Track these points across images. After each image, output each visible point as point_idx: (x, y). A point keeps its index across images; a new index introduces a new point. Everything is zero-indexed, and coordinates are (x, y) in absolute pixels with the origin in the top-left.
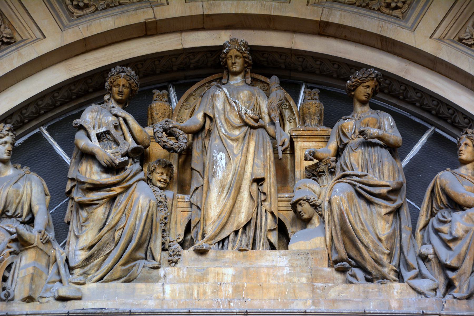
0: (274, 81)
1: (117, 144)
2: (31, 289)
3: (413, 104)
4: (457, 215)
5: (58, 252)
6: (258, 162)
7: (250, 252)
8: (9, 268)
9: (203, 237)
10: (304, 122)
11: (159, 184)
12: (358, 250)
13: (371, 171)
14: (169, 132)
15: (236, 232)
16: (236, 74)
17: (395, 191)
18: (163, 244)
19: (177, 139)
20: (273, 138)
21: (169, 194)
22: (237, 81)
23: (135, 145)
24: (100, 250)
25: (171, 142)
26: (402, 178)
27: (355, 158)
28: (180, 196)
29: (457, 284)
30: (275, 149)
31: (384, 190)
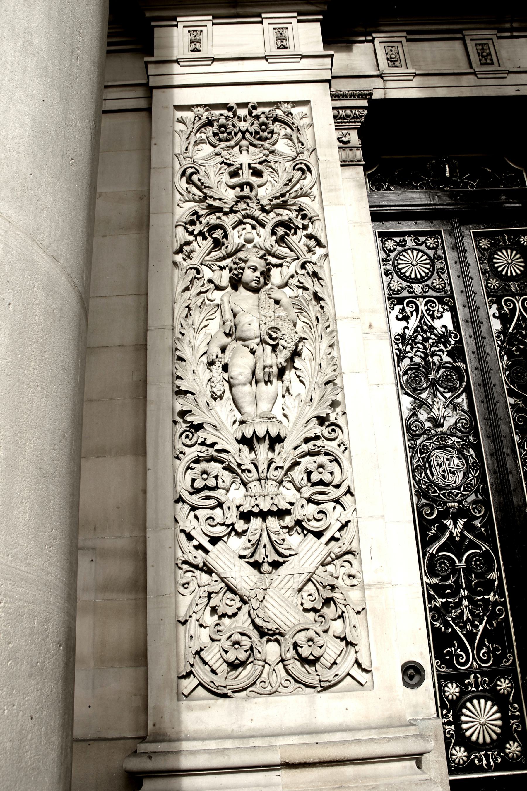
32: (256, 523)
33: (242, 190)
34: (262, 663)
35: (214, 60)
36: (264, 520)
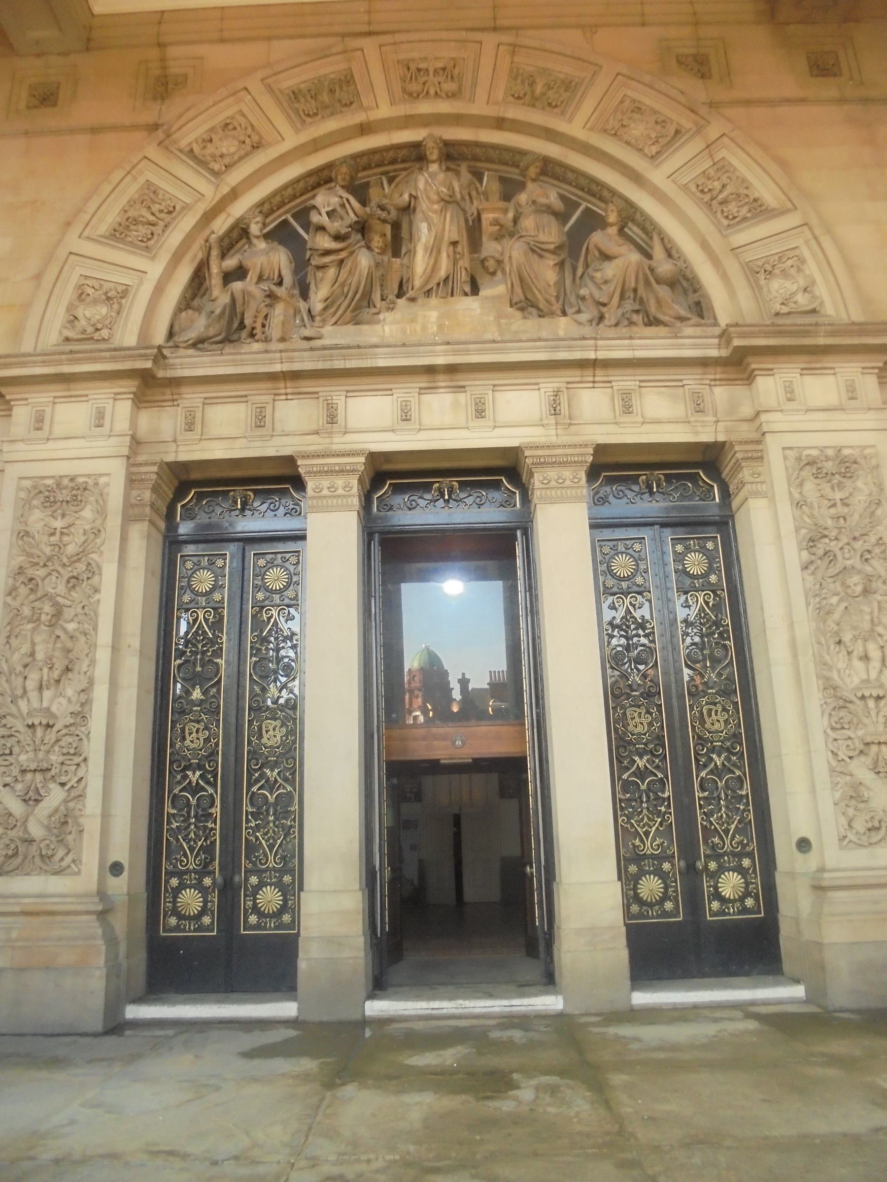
0: (464, 168)
1: (342, 218)
2: (283, 332)
3: (570, 184)
4: (606, 264)
5: (302, 305)
6: (454, 229)
7: (450, 299)
8: (266, 317)
9: (412, 289)
10: (487, 199)
11: (376, 250)
12: (533, 293)
13: (541, 232)
14: (382, 208)
15: (438, 284)
16: (433, 162)
17: (560, 248)
18: (382, 296)
19: (389, 213)
20: (464, 211)
21: (386, 258)
22: (434, 167)
23: (356, 219)
24: (333, 302)
25: (384, 215)
26: (565, 238)
27: (528, 223)
28: (394, 259)
29: (607, 316)
30: (466, 221)
31: (552, 247)
35: (807, 411)
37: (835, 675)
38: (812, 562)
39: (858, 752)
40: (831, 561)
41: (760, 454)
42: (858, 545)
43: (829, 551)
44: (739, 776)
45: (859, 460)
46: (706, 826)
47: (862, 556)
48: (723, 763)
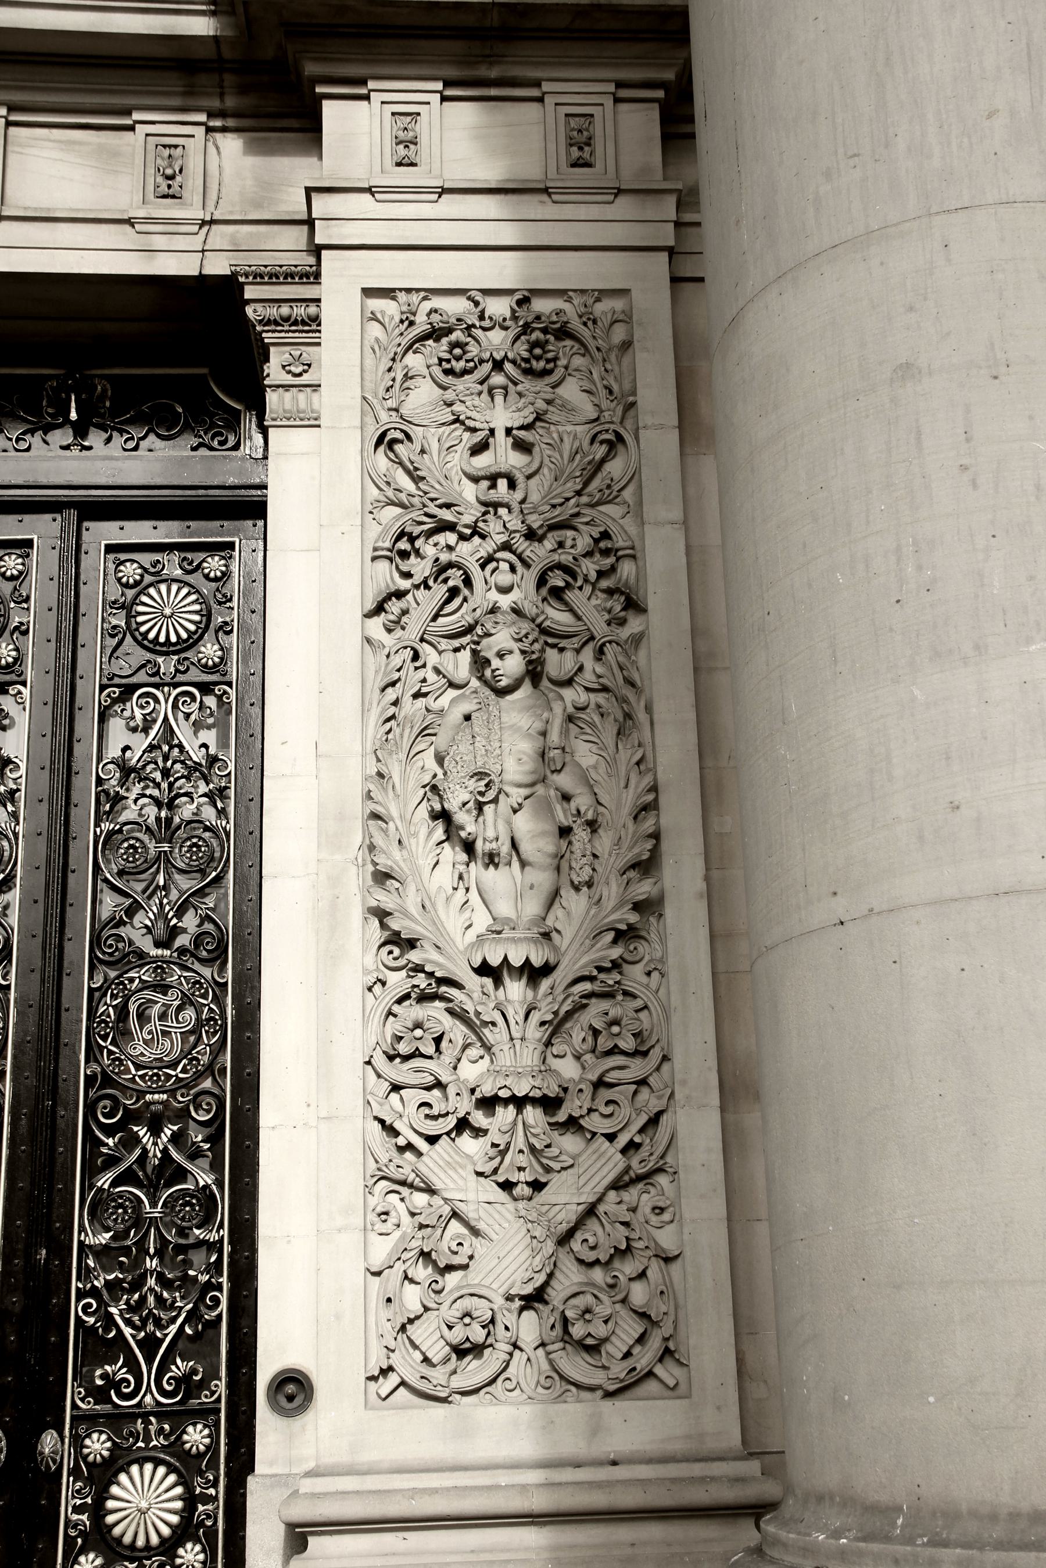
32: (506, 1115)
33: (493, 486)
34: (510, 1348)
35: (444, 191)
36: (520, 1109)
37: (412, 903)
38: (400, 595)
39: (451, 1122)
40: (454, 592)
41: (312, 310)
42: (540, 553)
43: (450, 565)
44: (206, 1186)
45: (576, 325)
46: (93, 1329)
47: (542, 581)
48: (165, 1151)
